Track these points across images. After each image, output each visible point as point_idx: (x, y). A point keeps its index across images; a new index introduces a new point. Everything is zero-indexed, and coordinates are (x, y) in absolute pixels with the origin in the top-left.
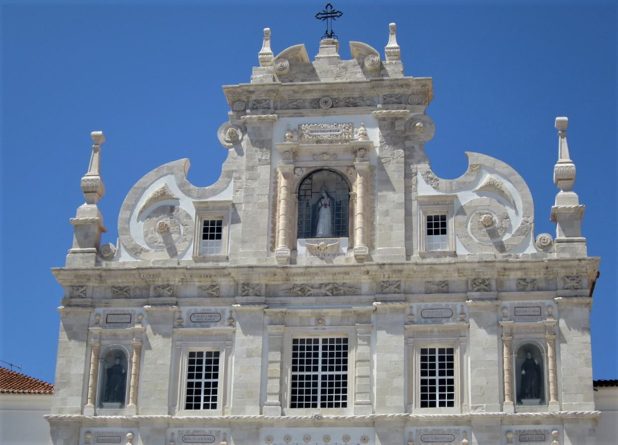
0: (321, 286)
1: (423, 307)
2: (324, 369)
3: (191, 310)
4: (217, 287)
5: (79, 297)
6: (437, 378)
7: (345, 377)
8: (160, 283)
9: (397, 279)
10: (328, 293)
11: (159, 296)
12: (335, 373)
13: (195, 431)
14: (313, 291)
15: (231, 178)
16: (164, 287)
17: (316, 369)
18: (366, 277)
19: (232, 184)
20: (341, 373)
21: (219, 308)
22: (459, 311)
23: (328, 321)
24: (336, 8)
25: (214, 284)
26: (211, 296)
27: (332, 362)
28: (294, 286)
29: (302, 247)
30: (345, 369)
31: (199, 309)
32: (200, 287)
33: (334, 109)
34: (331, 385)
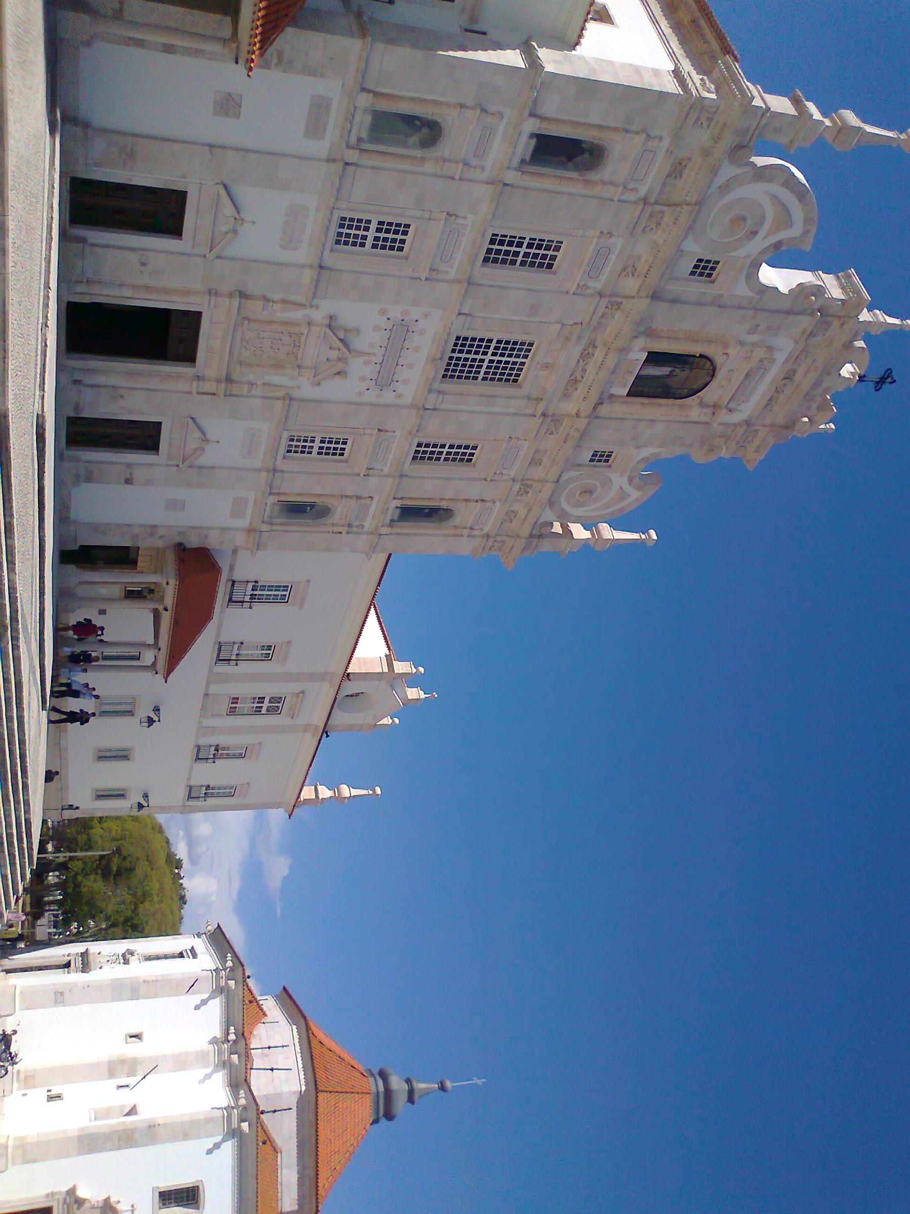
0: (584, 370)
4: (630, 276)
5: (698, 119)
8: (665, 219)
9: (560, 432)
10: (573, 377)
11: (650, 216)
13: (461, 242)
14: (582, 364)
15: (757, 294)
16: (658, 224)
18: (574, 412)
19: (751, 294)
21: (603, 278)
22: (505, 472)
23: (543, 373)
24: (887, 387)
25: (636, 274)
26: (624, 269)
28: (595, 347)
31: (613, 257)
32: (639, 257)
33: (774, 389)
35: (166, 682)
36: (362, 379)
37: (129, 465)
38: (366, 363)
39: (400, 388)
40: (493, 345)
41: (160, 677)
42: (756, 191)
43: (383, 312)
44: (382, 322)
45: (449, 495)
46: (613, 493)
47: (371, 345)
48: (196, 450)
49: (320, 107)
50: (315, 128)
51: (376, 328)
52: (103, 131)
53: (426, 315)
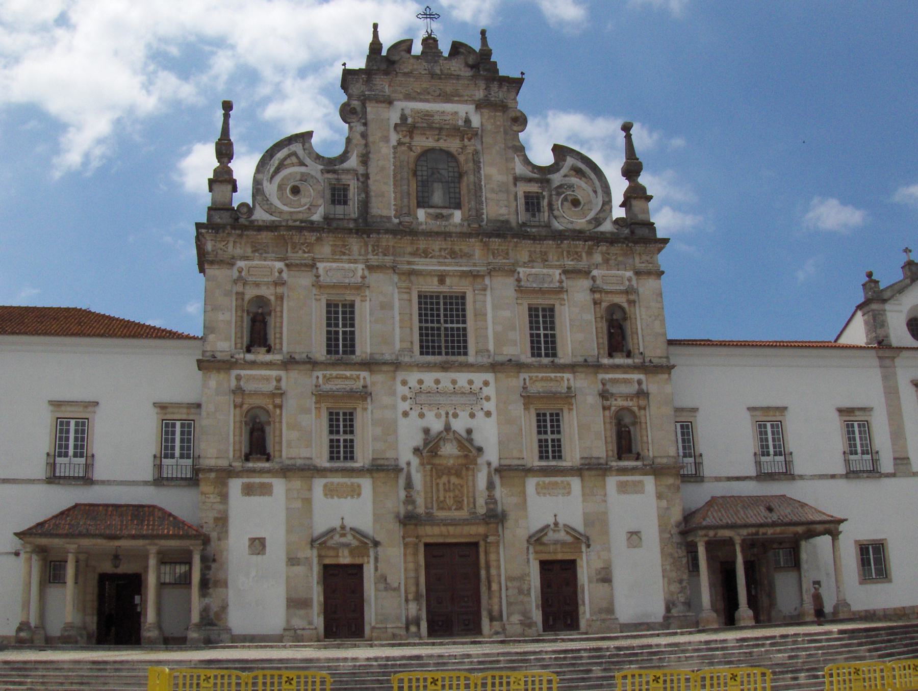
1: (528, 273)
2: (446, 322)
3: (325, 267)
6: (542, 332)
7: (465, 329)
12: (455, 325)
17: (439, 322)
20: (461, 326)
27: (452, 316)
29: (421, 214)
30: (464, 322)
34: (453, 336)
35: (846, 520)
36: (472, 416)
37: (590, 582)
38: (455, 416)
39: (478, 383)
40: (424, 325)
41: (842, 527)
42: (271, 189)
43: (406, 414)
44: (414, 414)
45: (589, 316)
46: (574, 180)
47: (438, 416)
48: (568, 533)
49: (248, 490)
50: (265, 490)
51: (422, 415)
52: (288, 621)
53: (404, 383)
